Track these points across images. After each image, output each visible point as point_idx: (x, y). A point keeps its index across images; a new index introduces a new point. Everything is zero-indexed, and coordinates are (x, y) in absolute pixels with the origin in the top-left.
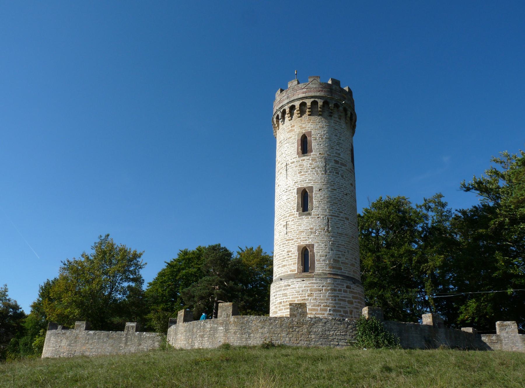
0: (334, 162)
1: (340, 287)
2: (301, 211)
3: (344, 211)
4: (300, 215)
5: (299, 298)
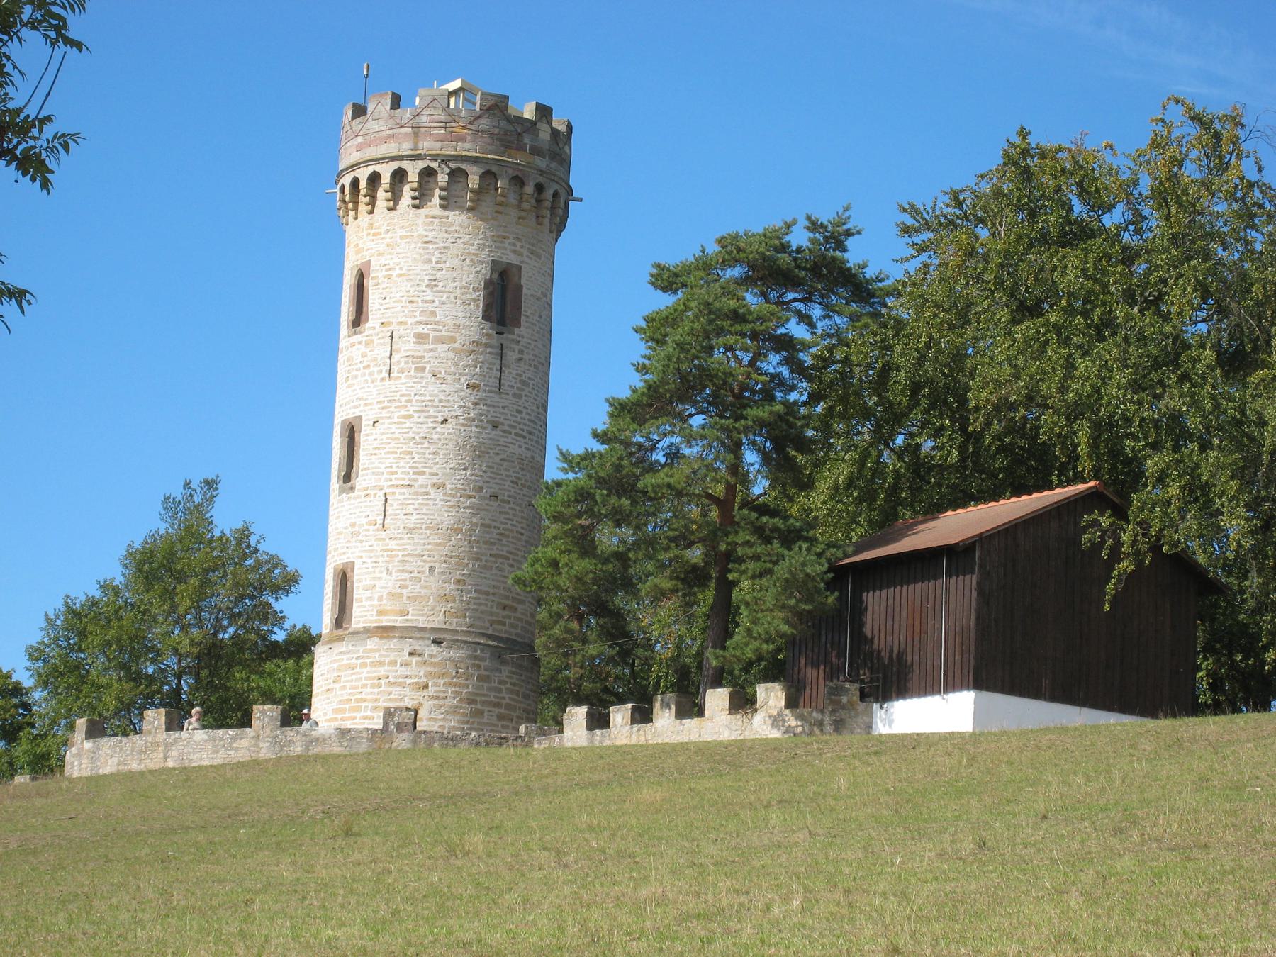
0: (413, 339)
1: (392, 656)
2: (341, 482)
3: (432, 468)
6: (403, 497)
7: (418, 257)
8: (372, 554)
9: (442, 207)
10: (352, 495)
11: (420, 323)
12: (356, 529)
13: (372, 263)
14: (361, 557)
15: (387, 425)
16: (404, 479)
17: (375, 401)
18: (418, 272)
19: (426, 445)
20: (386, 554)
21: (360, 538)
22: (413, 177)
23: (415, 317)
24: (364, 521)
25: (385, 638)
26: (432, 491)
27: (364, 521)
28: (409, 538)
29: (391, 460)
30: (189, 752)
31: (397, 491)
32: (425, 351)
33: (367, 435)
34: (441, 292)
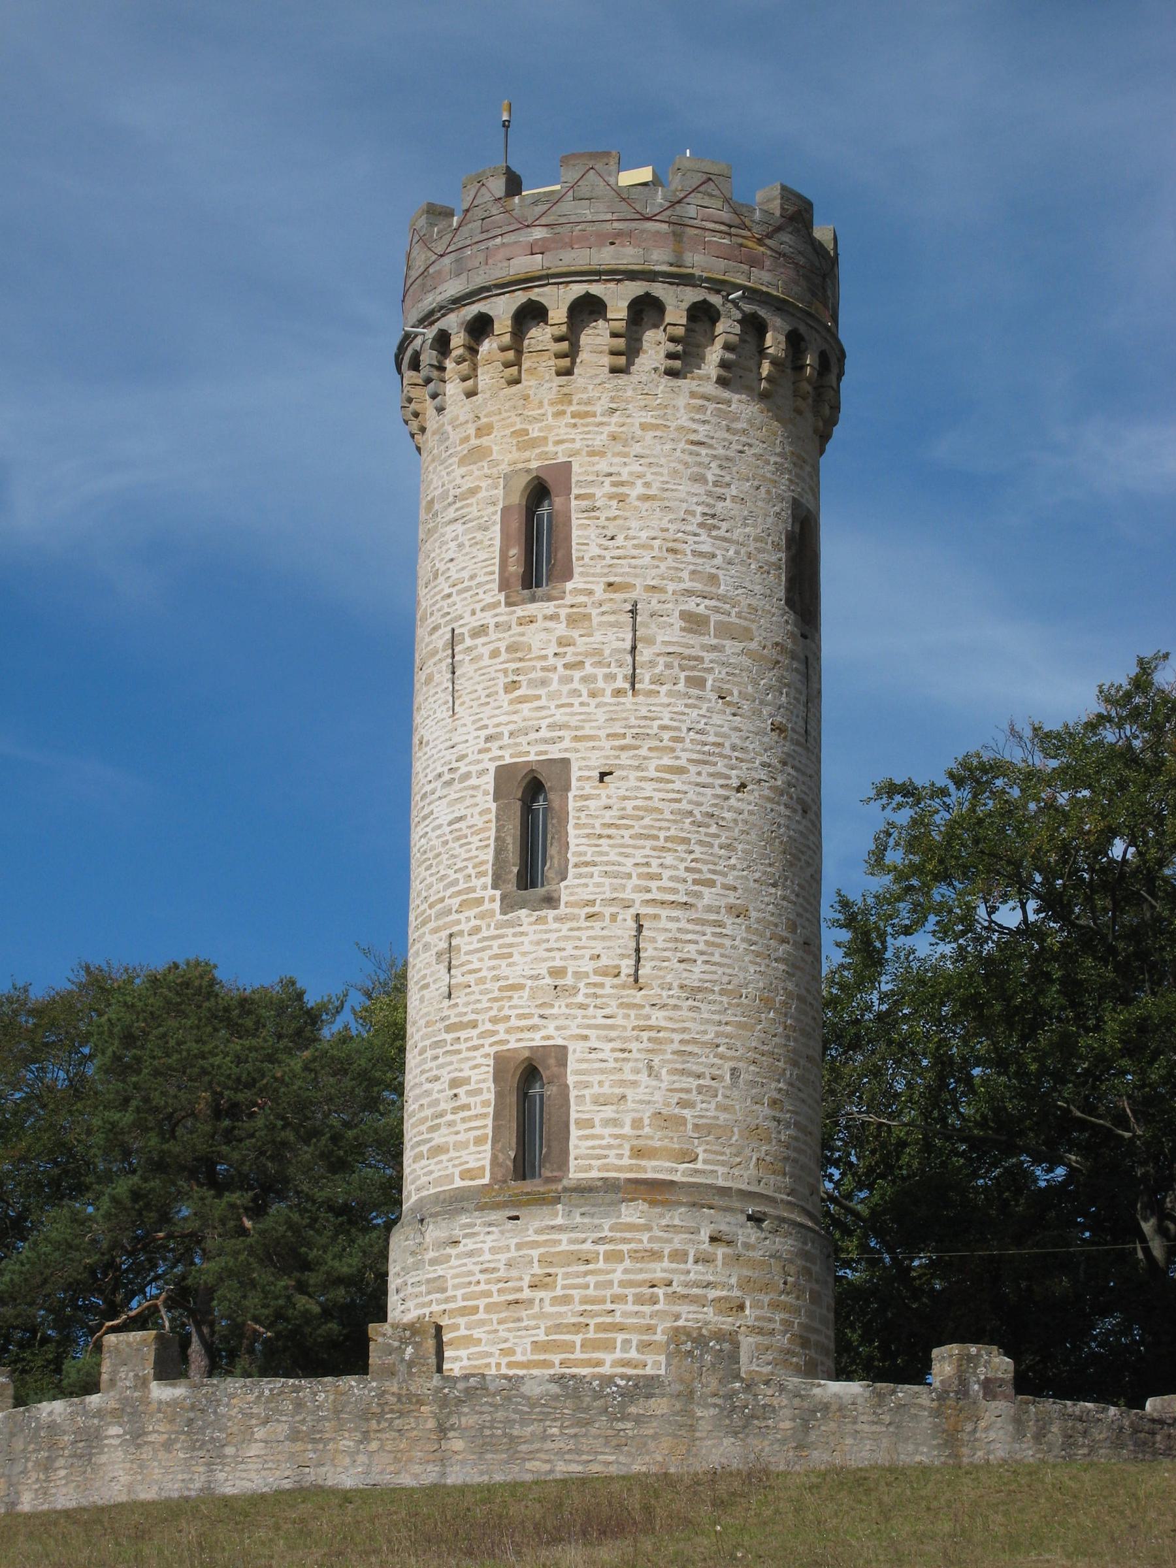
1: (678, 1241)
2: (511, 887)
3: (725, 875)
4: (508, 905)
5: (496, 1298)
6: (673, 926)
7: (680, 467)
8: (613, 1034)
9: (722, 382)
10: (551, 914)
11: (689, 593)
12: (569, 980)
13: (575, 468)
14: (585, 1038)
15: (633, 783)
16: (675, 891)
17: (602, 733)
18: (683, 495)
19: (713, 829)
20: (645, 1035)
21: (580, 998)
22: (676, 314)
23: (681, 580)
24: (587, 966)
25: (662, 1203)
26: (729, 921)
27: (587, 966)
28: (691, 1009)
29: (647, 852)
30: (509, 1422)
31: (664, 913)
32: (703, 647)
33: (586, 798)
34: (725, 539)
